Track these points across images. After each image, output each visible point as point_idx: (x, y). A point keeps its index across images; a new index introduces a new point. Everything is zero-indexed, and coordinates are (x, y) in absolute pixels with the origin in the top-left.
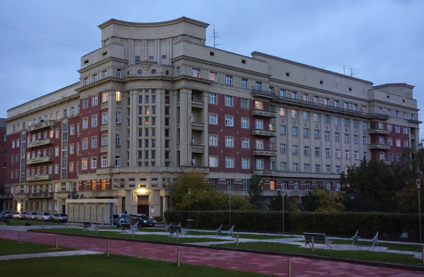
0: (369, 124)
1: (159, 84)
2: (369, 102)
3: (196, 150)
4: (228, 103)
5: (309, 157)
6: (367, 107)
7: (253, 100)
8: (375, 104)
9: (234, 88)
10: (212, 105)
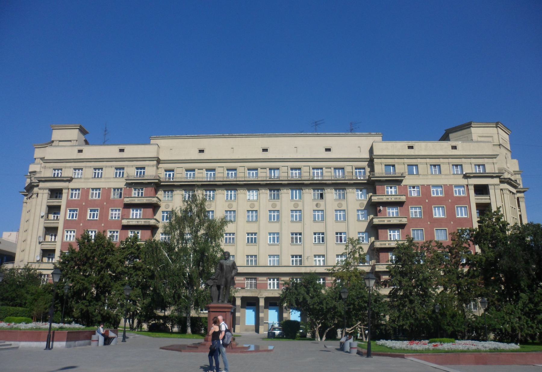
3: (48, 246)
5: (256, 246)
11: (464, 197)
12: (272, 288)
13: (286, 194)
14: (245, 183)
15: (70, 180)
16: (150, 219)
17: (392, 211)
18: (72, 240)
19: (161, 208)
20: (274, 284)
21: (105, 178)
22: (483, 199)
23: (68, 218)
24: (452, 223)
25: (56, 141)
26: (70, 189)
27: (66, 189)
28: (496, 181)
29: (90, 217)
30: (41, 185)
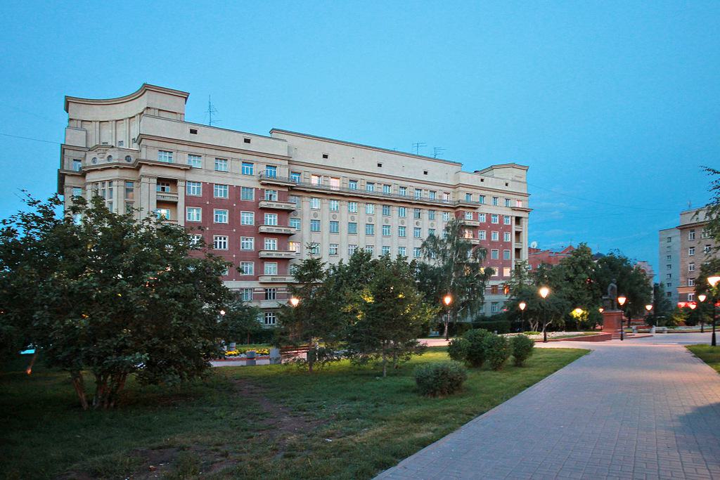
0: (453, 214)
1: (115, 174)
2: (455, 187)
4: (220, 194)
8: (461, 188)
9: (229, 175)
10: (191, 197)
13: (395, 210)
15: (188, 169)
27: (182, 181)
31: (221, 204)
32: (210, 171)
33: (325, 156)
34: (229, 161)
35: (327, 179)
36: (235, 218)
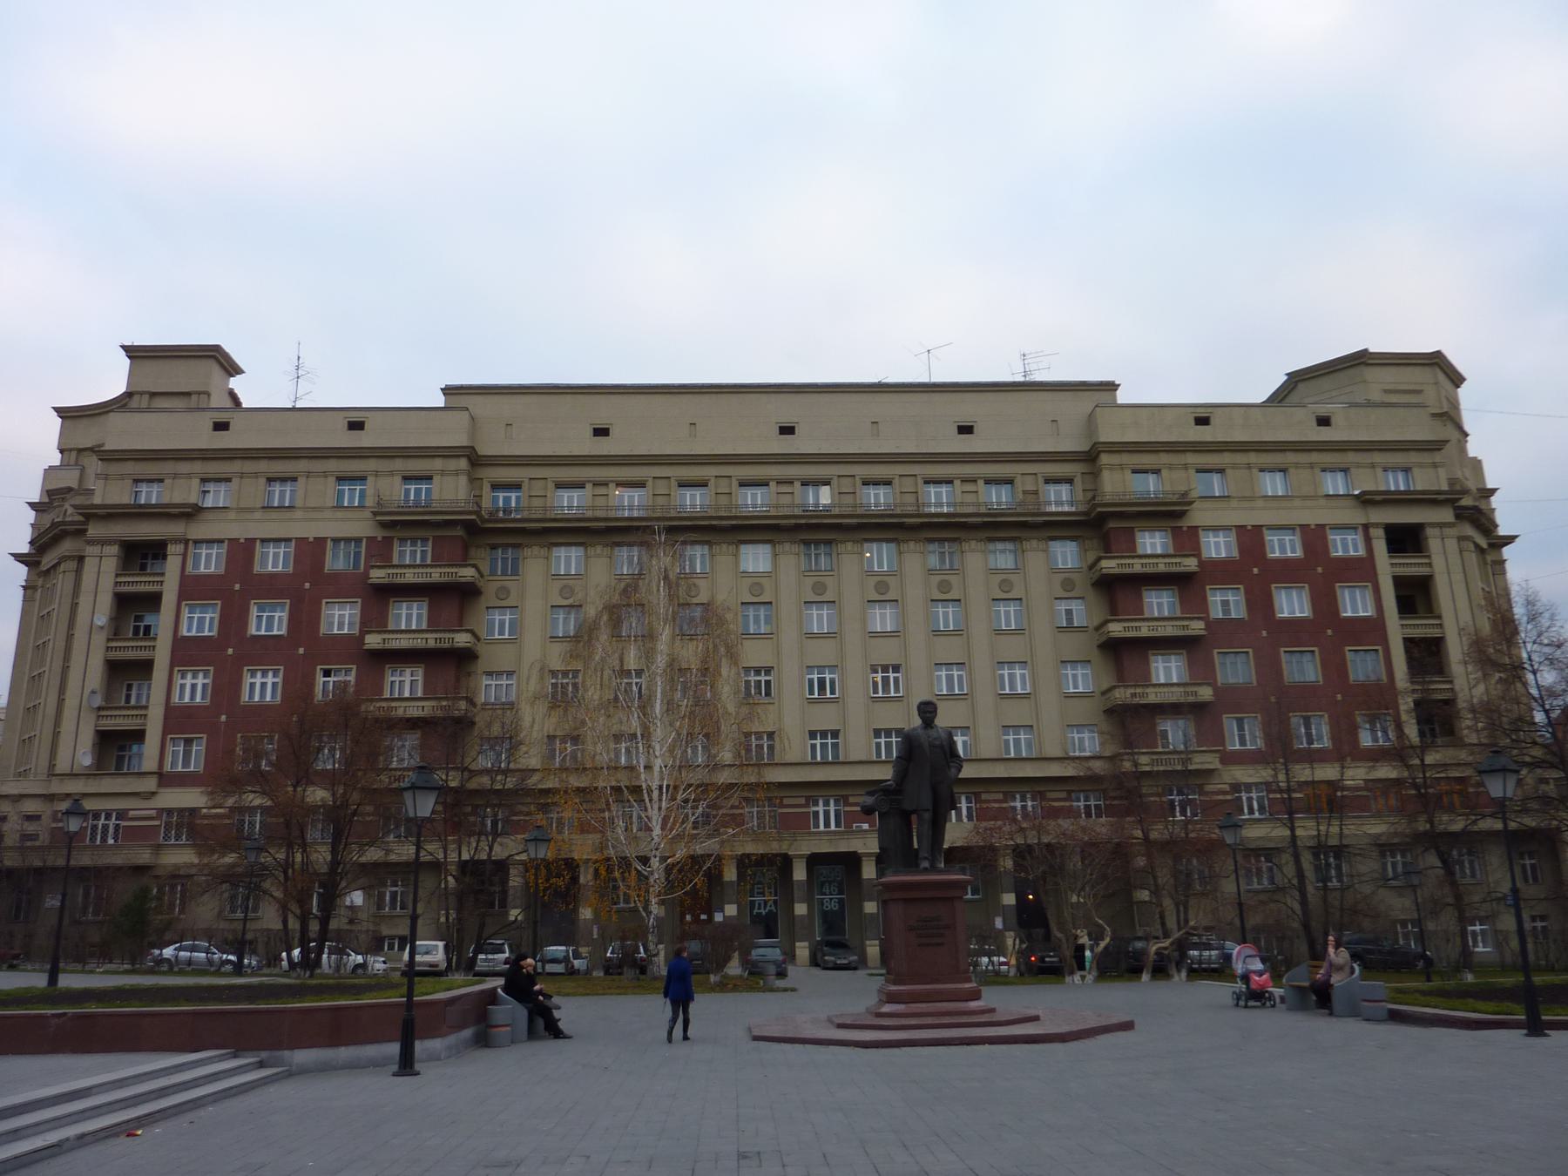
6: (1078, 481)
7: (384, 537)
9: (298, 514)
11: (1359, 560)
12: (822, 828)
14: (734, 522)
15: (191, 513)
16: (453, 631)
17: (1159, 603)
18: (198, 699)
19: (483, 598)
20: (827, 814)
21: (305, 509)
22: (1411, 566)
23: (185, 633)
24: (1329, 632)
25: (141, 393)
26: (191, 542)
27: (176, 541)
28: (1446, 515)
29: (259, 628)
30: (94, 530)
31: (271, 588)
32: (251, 510)
33: (601, 432)
34: (301, 480)
35: (602, 490)
36: (304, 619)
